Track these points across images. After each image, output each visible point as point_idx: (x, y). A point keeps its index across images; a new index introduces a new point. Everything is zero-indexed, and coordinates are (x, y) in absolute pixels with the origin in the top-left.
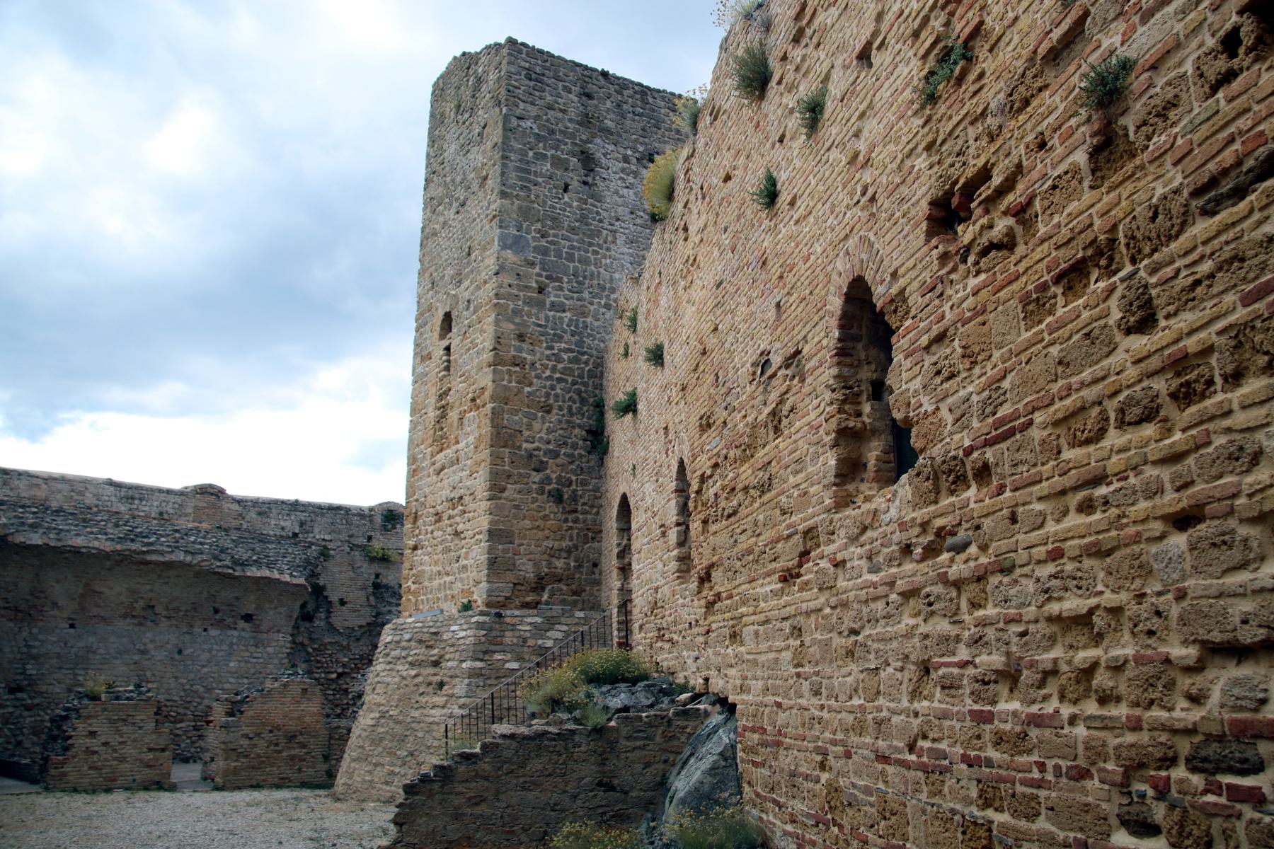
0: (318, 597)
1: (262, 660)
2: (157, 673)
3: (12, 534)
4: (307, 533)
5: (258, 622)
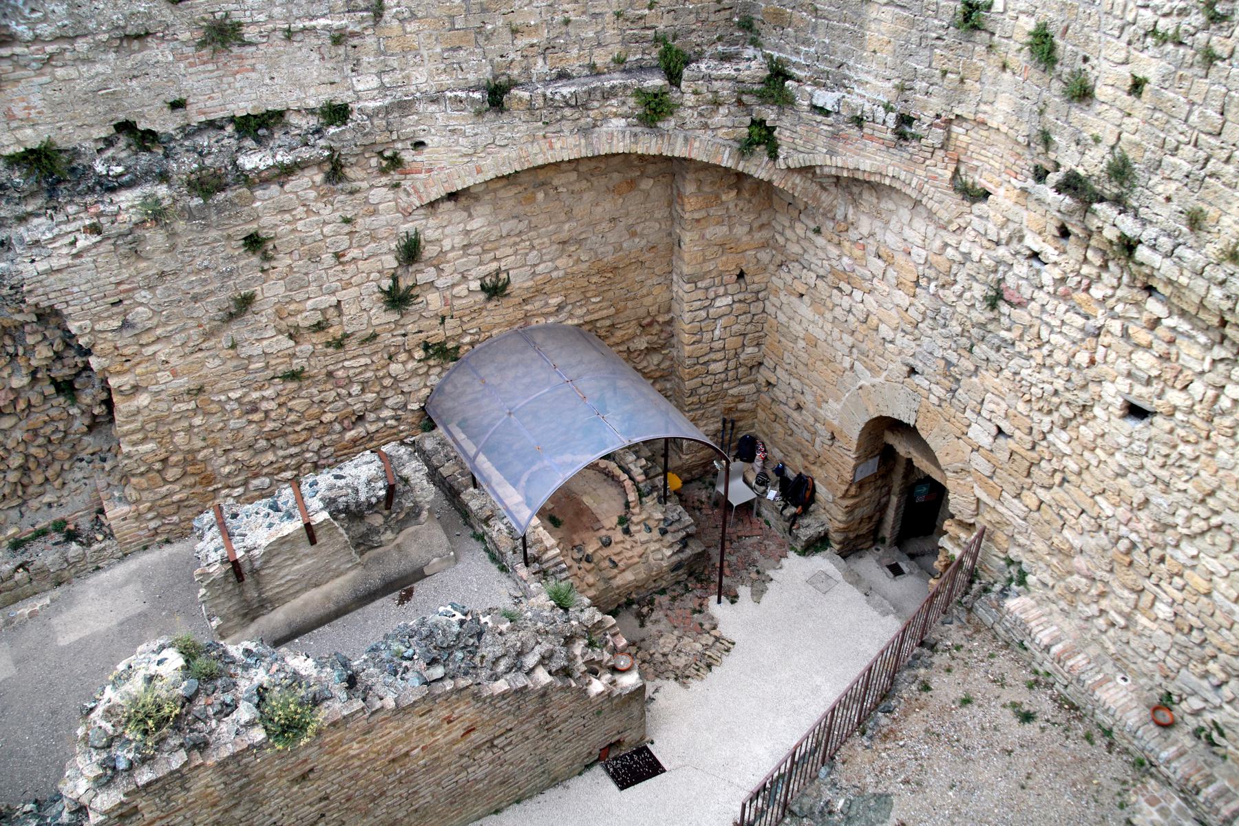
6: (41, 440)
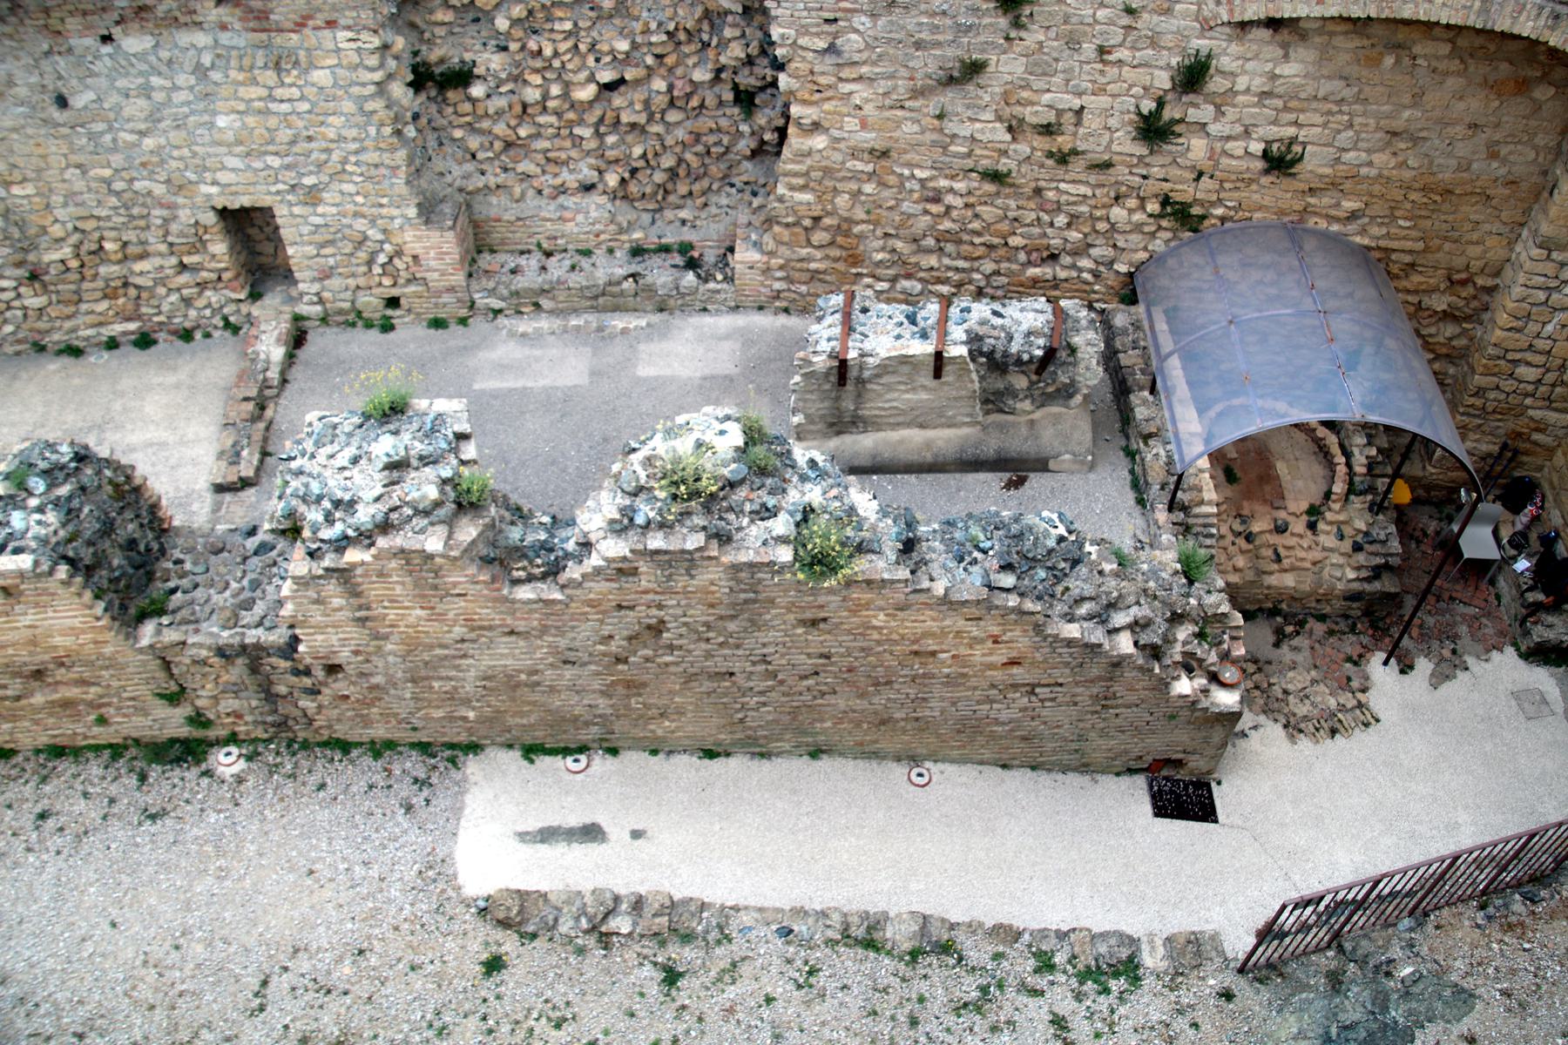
1: (305, 106)
6: (700, 148)
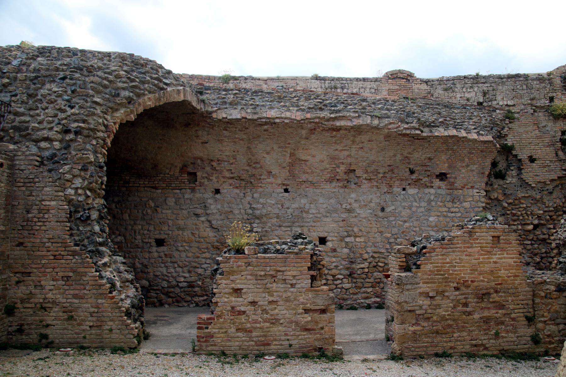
0: (507, 157)
1: (459, 215)
2: (363, 229)
3: (216, 111)
4: (491, 101)
5: (452, 180)
